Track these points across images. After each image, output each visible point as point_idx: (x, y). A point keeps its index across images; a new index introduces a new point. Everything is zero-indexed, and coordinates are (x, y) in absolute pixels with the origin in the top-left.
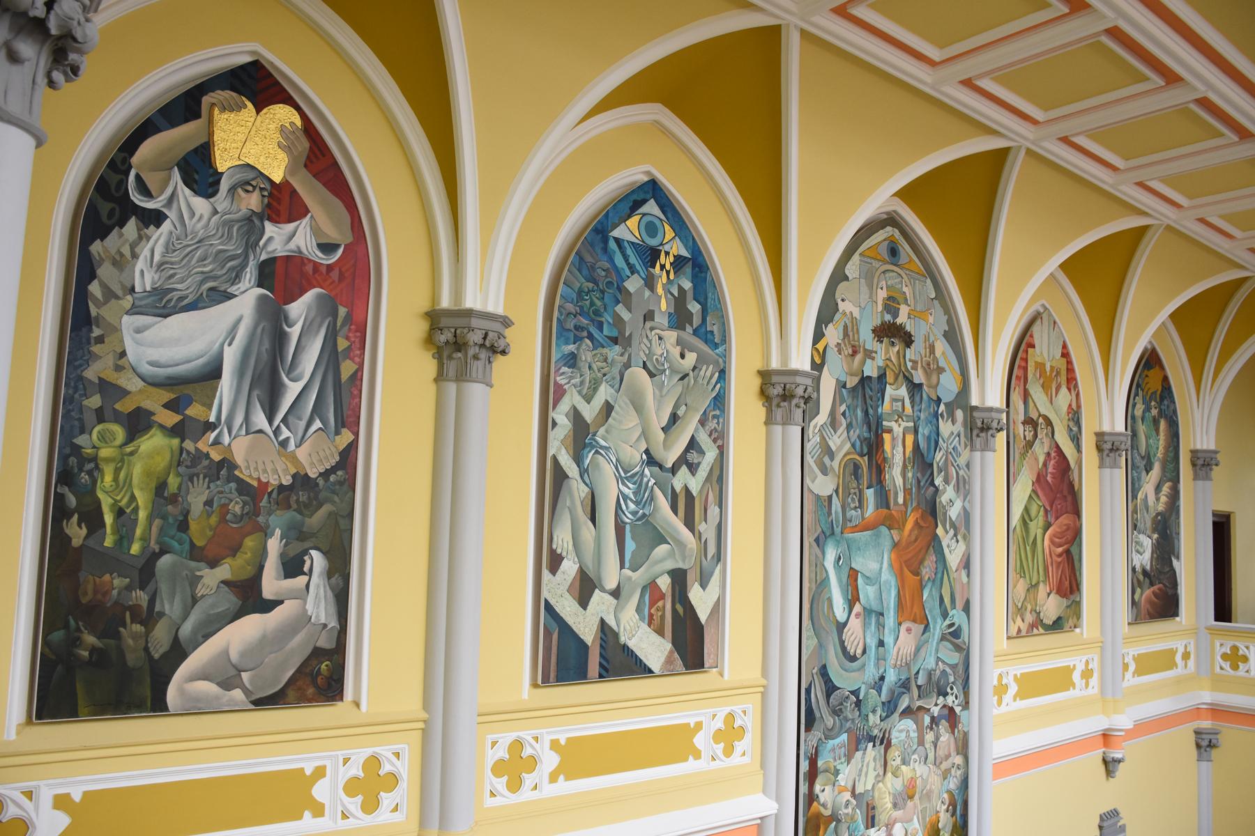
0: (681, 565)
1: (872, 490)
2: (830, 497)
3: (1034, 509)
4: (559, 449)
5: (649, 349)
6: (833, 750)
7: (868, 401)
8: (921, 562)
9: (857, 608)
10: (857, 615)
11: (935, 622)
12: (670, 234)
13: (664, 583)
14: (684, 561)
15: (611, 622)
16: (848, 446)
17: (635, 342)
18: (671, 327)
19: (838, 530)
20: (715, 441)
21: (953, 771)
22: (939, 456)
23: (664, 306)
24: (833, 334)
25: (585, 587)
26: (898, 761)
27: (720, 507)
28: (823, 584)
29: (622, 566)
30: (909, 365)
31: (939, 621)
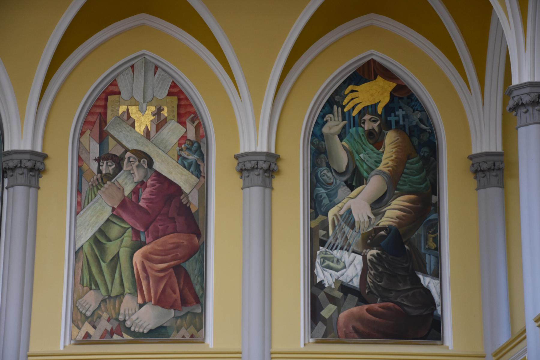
3: (114, 231)
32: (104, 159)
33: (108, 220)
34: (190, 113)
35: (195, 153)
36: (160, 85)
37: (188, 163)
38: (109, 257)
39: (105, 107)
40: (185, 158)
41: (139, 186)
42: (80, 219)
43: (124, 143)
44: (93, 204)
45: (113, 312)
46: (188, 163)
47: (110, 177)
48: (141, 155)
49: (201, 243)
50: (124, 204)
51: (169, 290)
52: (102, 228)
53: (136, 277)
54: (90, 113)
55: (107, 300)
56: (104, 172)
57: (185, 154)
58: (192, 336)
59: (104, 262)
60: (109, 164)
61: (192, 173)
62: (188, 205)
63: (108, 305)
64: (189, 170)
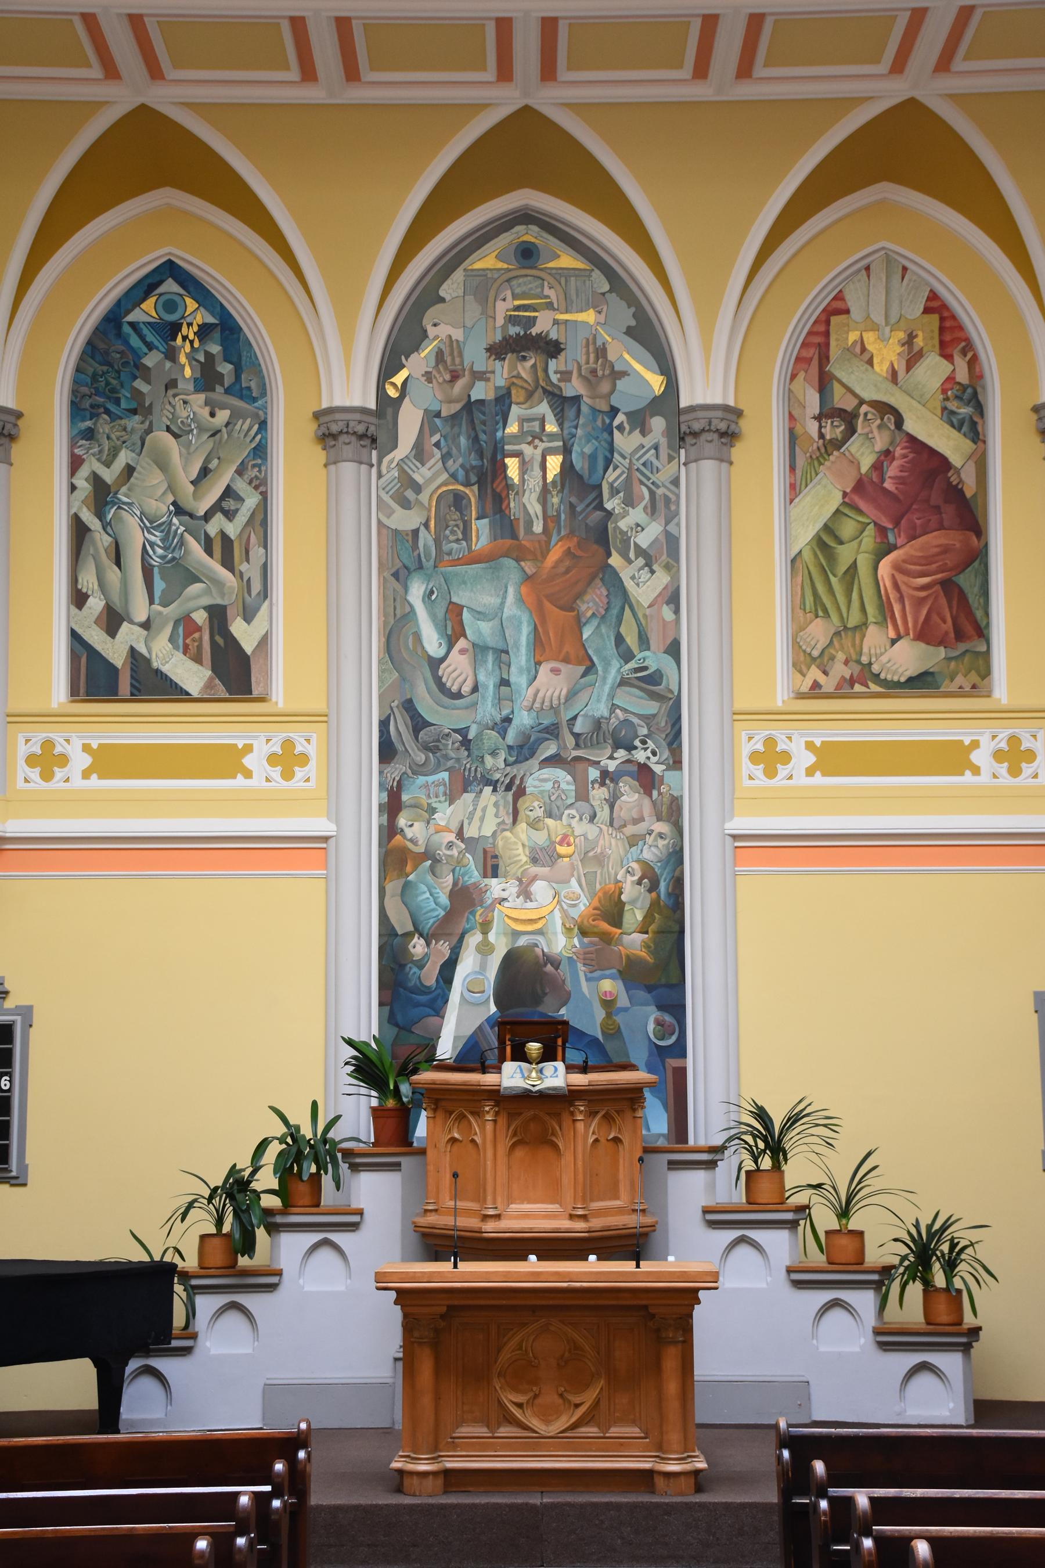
0: (219, 601)
1: (486, 521)
2: (416, 532)
3: (848, 528)
4: (80, 508)
5: (173, 414)
6: (426, 786)
7: (479, 427)
8: (580, 595)
9: (462, 643)
10: (462, 651)
11: (607, 664)
12: (191, 304)
13: (200, 617)
14: (222, 595)
15: (142, 649)
16: (445, 476)
17: (156, 410)
18: (197, 390)
19: (428, 564)
20: (256, 488)
21: (650, 840)
22: (611, 475)
23: (188, 372)
24: (417, 364)
25: (113, 620)
26: (540, 813)
27: (265, 547)
28: (409, 616)
29: (151, 602)
30: (554, 378)
31: (616, 664)
32: (829, 416)
33: (837, 511)
34: (959, 340)
35: (968, 403)
36: (911, 296)
37: (959, 420)
38: (842, 568)
39: (827, 334)
40: (953, 413)
41: (882, 458)
42: (795, 510)
43: (858, 391)
44: (814, 487)
45: (852, 651)
46: (959, 420)
47: (837, 444)
48: (884, 409)
49: (982, 543)
50: (860, 486)
51: (935, 618)
52: (830, 525)
53: (884, 598)
54: (804, 345)
55: (843, 633)
56: (828, 437)
57: (953, 405)
58: (974, 687)
59: (835, 576)
60: (835, 424)
61: (965, 435)
62: (960, 487)
63: (843, 641)
64: (959, 430)
